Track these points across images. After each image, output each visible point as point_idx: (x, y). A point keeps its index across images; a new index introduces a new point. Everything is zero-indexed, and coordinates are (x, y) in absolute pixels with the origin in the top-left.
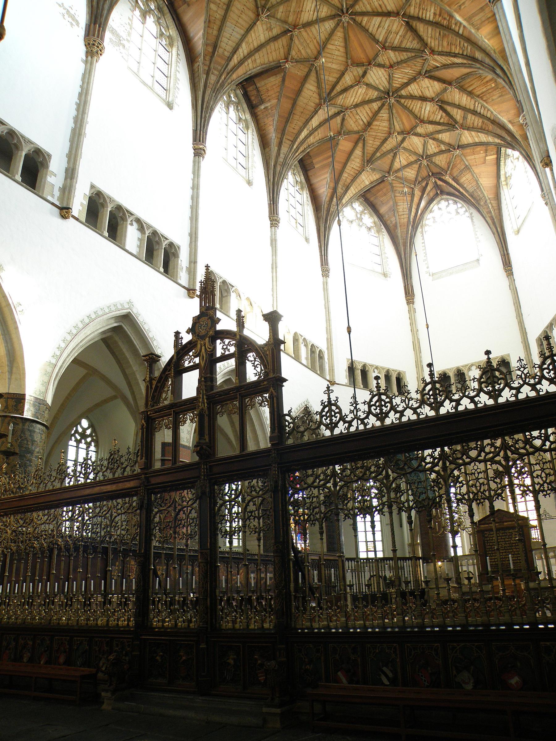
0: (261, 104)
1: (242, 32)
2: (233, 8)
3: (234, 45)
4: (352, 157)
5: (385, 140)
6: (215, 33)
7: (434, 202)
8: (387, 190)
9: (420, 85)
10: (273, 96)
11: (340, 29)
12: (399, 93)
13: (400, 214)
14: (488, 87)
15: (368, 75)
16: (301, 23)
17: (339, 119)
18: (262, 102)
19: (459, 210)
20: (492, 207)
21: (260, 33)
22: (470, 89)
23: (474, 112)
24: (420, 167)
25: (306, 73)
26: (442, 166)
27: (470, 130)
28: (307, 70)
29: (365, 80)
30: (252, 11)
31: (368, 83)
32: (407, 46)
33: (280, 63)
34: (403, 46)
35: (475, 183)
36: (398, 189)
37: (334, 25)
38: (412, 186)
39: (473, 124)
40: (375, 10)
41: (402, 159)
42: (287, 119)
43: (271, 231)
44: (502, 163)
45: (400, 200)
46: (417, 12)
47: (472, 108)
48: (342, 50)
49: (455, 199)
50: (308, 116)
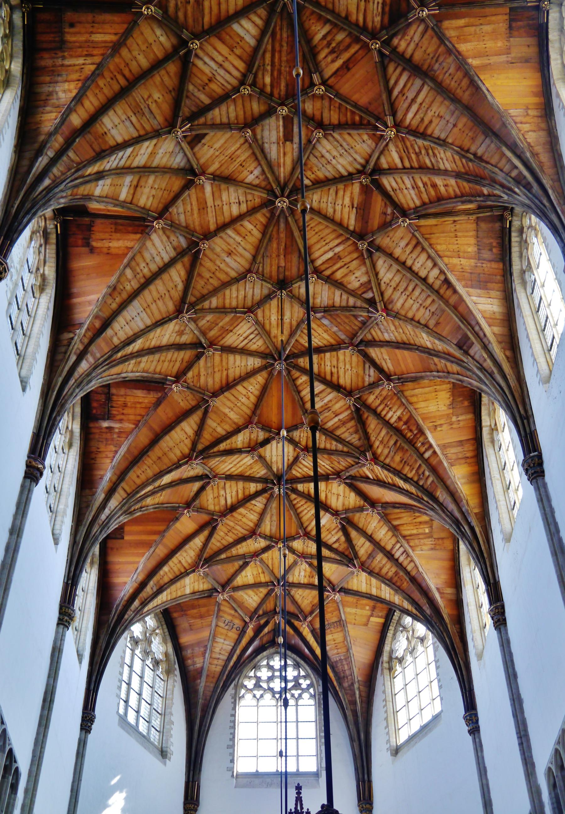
0: (104, 419)
1: (149, 322)
2: (152, 287)
3: (131, 333)
4: (187, 547)
5: (243, 539)
6: (114, 306)
7: (265, 653)
8: (208, 611)
9: (329, 488)
10: (132, 417)
11: (264, 374)
12: (294, 486)
13: (214, 656)
14: (420, 531)
15: (268, 447)
16: (221, 343)
17: (197, 485)
18: (109, 416)
19: (301, 681)
20: (360, 695)
21: (167, 334)
22: (396, 523)
23: (389, 555)
24: (268, 594)
25: (190, 407)
26: (303, 606)
27: (372, 576)
28: (194, 403)
29: (261, 450)
30: (174, 303)
31: (263, 455)
32: (343, 436)
33: (167, 380)
34: (338, 433)
35: (344, 650)
36: (226, 616)
37: (260, 365)
38: (247, 620)
39: (381, 569)
40: (323, 375)
41: (249, 575)
42: (135, 459)
43: (57, 632)
44: (390, 634)
45: (222, 634)
46: (377, 404)
47: (389, 547)
48: (253, 399)
49: (298, 659)
50: (165, 467)
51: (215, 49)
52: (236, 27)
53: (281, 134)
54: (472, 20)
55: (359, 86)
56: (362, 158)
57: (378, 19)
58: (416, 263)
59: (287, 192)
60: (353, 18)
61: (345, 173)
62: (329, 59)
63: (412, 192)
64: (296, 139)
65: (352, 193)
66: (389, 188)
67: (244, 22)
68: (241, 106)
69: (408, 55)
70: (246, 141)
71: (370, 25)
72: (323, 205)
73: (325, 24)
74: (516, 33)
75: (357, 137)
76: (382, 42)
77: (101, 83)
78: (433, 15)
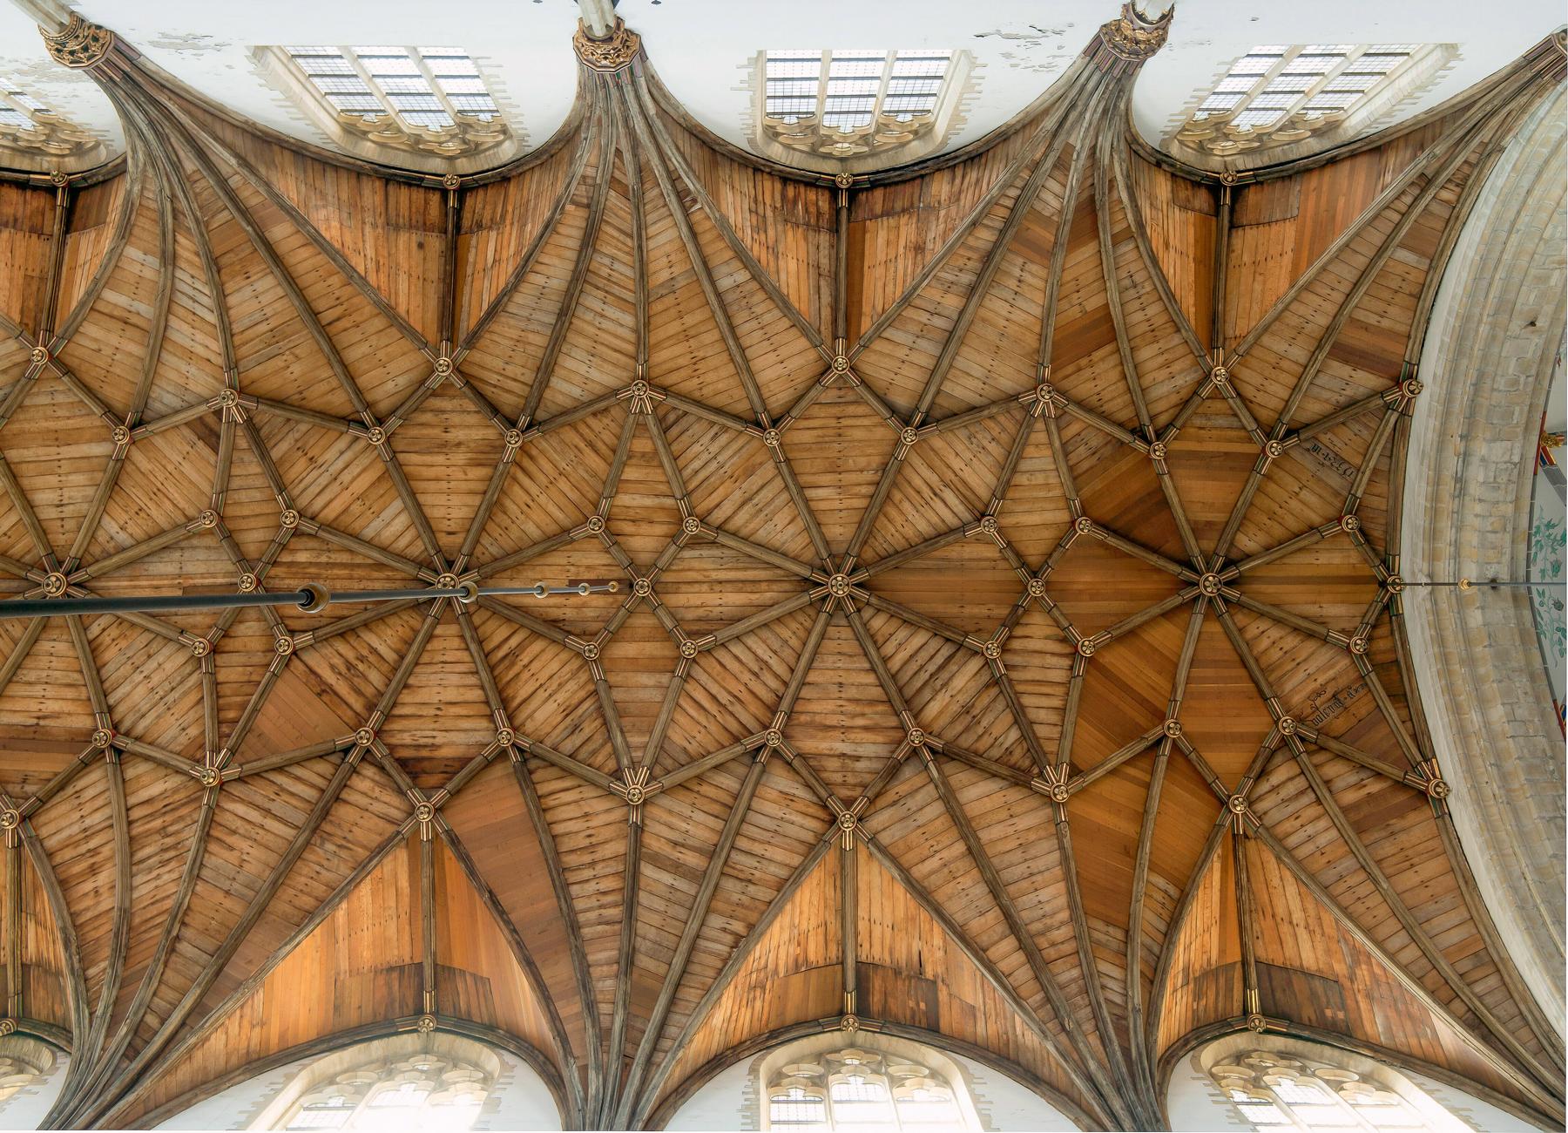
51: (364, 470)
52: (398, 505)
53: (198, 581)
54: (407, 900)
55: (291, 714)
56: (147, 729)
57: (407, 739)
60: (406, 697)
61: (111, 701)
62: (337, 661)
65: (69, 714)
66: (80, 784)
67: (403, 520)
68: (258, 511)
69: (344, 795)
70: (190, 520)
71: (396, 725)
72: (44, 661)
73: (397, 652)
74: (381, 980)
75: (192, 715)
76: (368, 751)
78: (417, 832)
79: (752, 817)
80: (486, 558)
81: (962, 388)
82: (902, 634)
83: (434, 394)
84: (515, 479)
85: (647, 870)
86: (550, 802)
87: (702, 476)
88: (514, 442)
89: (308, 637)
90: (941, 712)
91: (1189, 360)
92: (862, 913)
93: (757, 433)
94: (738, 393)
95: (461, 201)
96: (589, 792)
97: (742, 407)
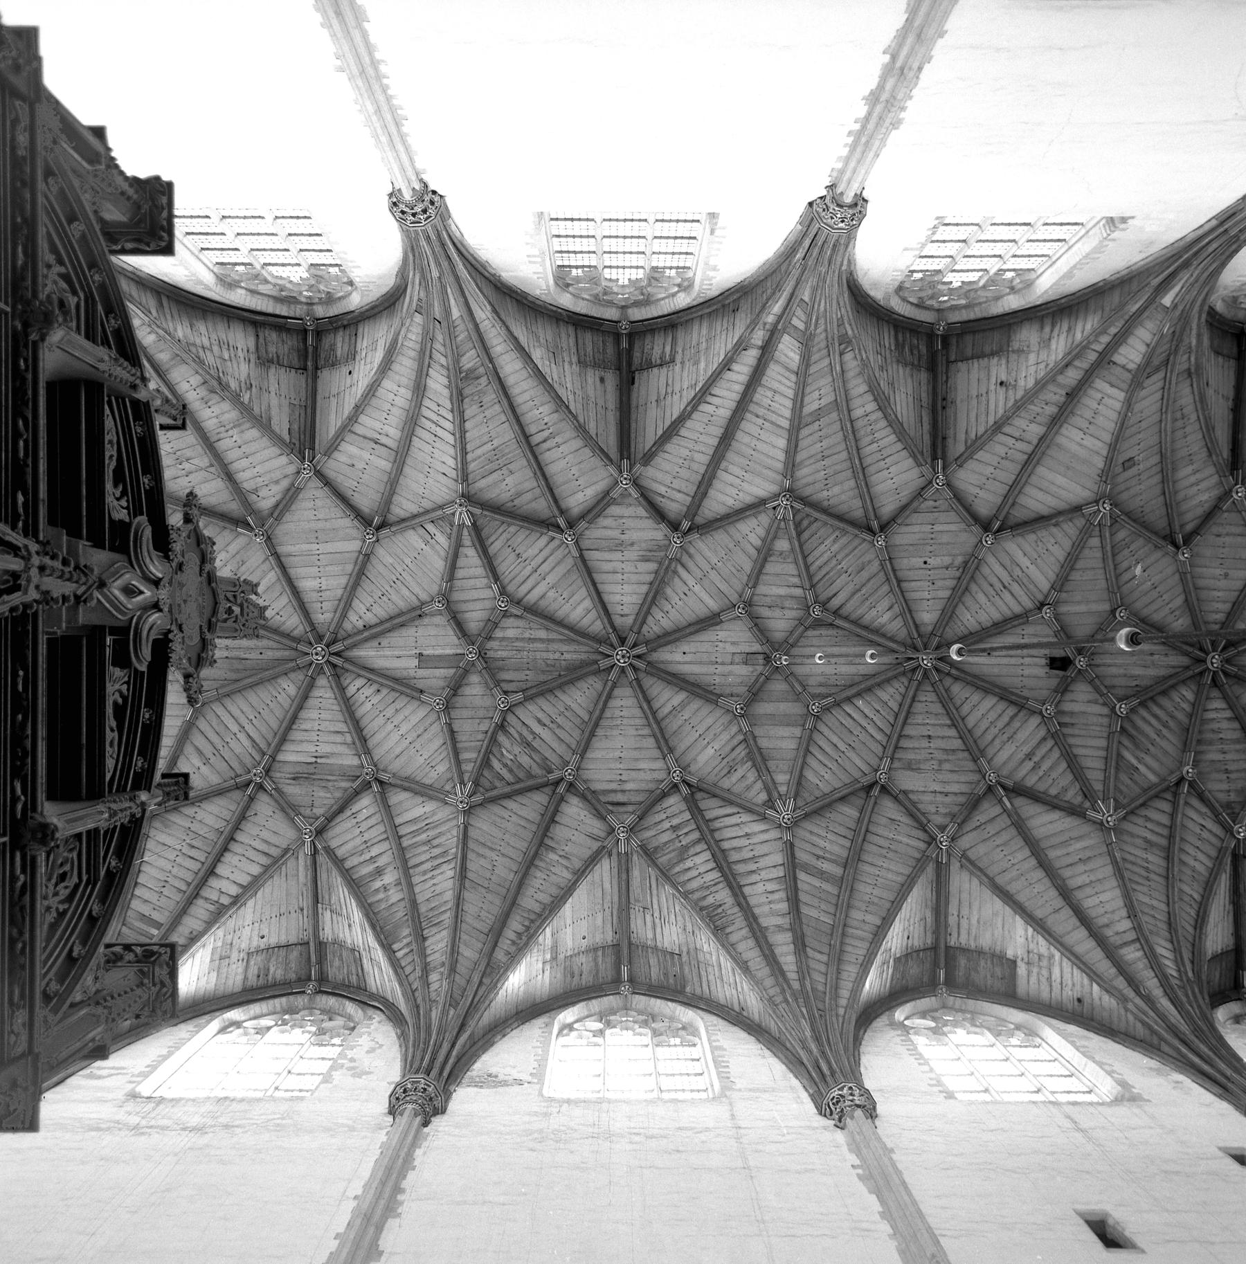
51: (558, 563)
58: (238, 858)
59: (334, 660)
63: (358, 841)
64: (422, 673)
66: (355, 808)
77: (545, 409)
79: (870, 837)
80: (651, 636)
81: (1035, 500)
82: (976, 697)
83: (614, 502)
84: (675, 572)
85: (802, 876)
86: (717, 824)
87: (823, 572)
88: (677, 540)
89: (520, 696)
90: (1010, 758)
91: (1215, 479)
92: (953, 909)
93: (869, 537)
94: (857, 503)
95: (631, 344)
96: (745, 817)
97: (858, 514)
